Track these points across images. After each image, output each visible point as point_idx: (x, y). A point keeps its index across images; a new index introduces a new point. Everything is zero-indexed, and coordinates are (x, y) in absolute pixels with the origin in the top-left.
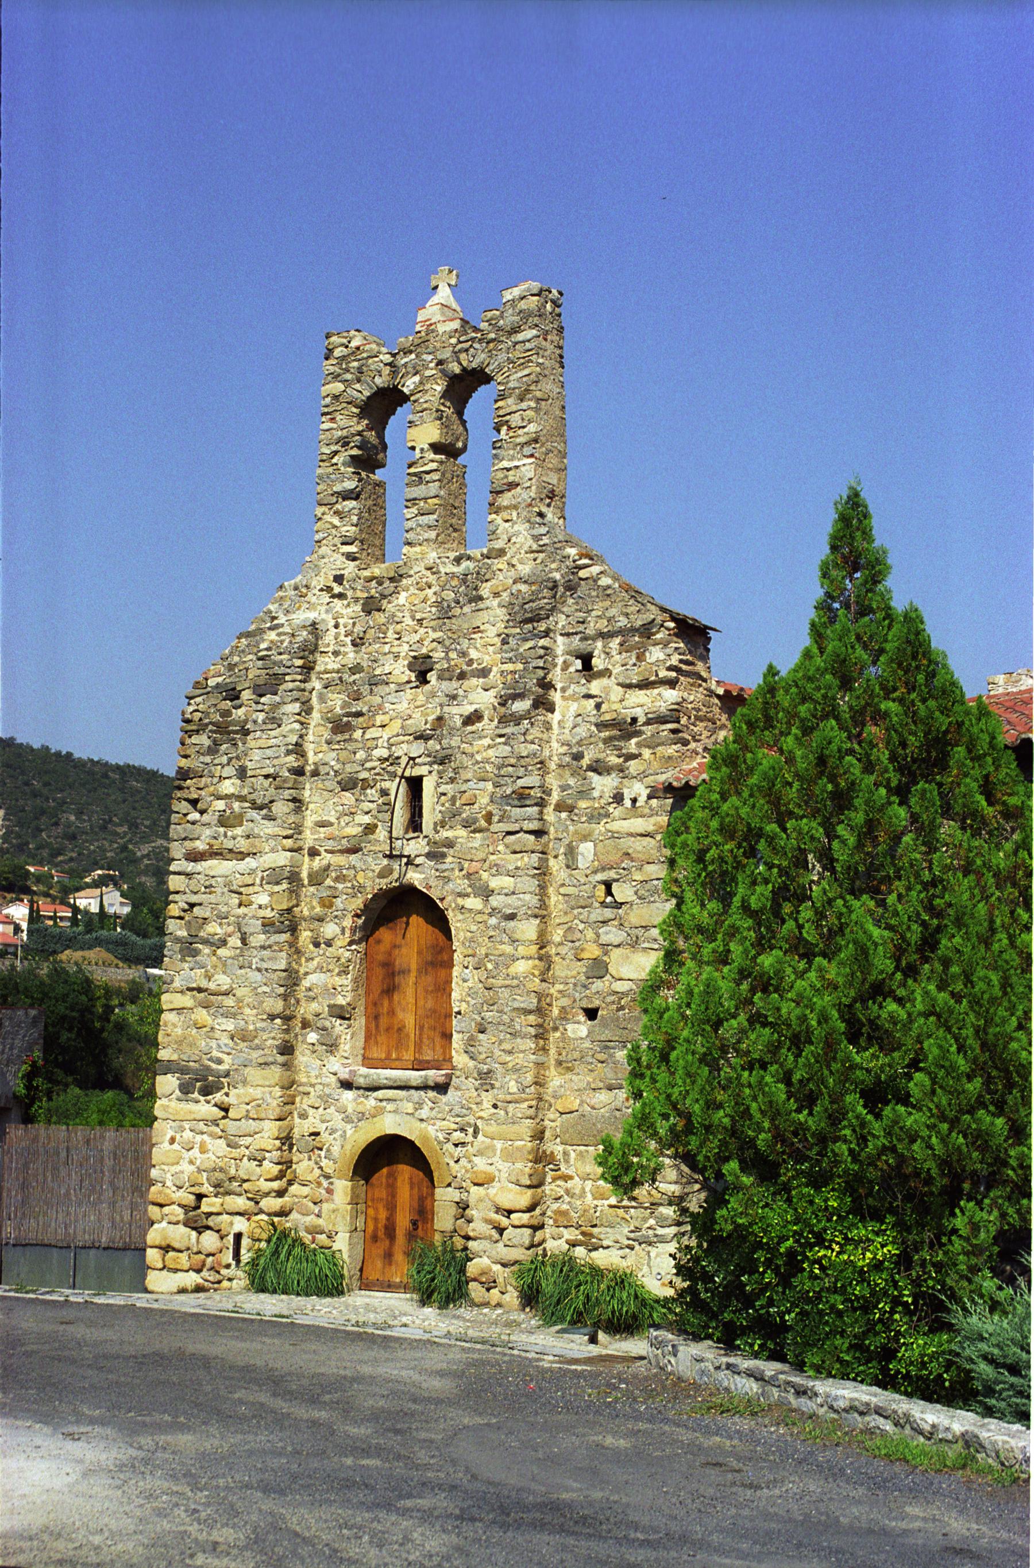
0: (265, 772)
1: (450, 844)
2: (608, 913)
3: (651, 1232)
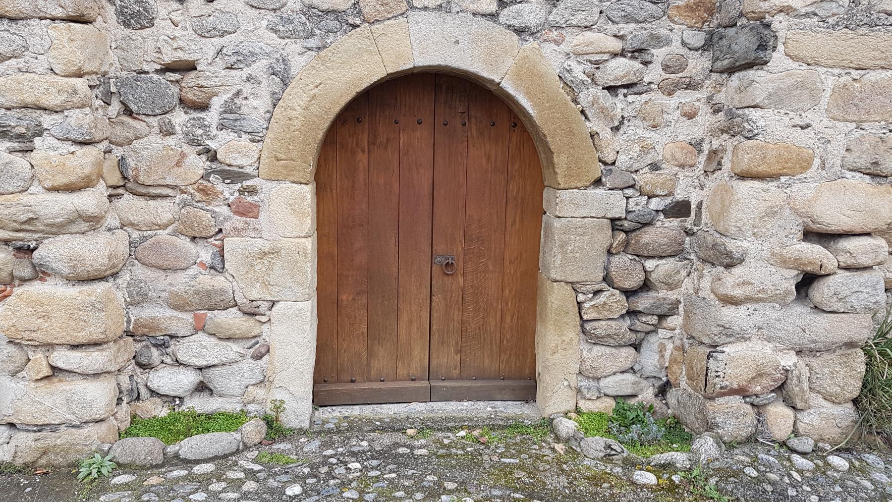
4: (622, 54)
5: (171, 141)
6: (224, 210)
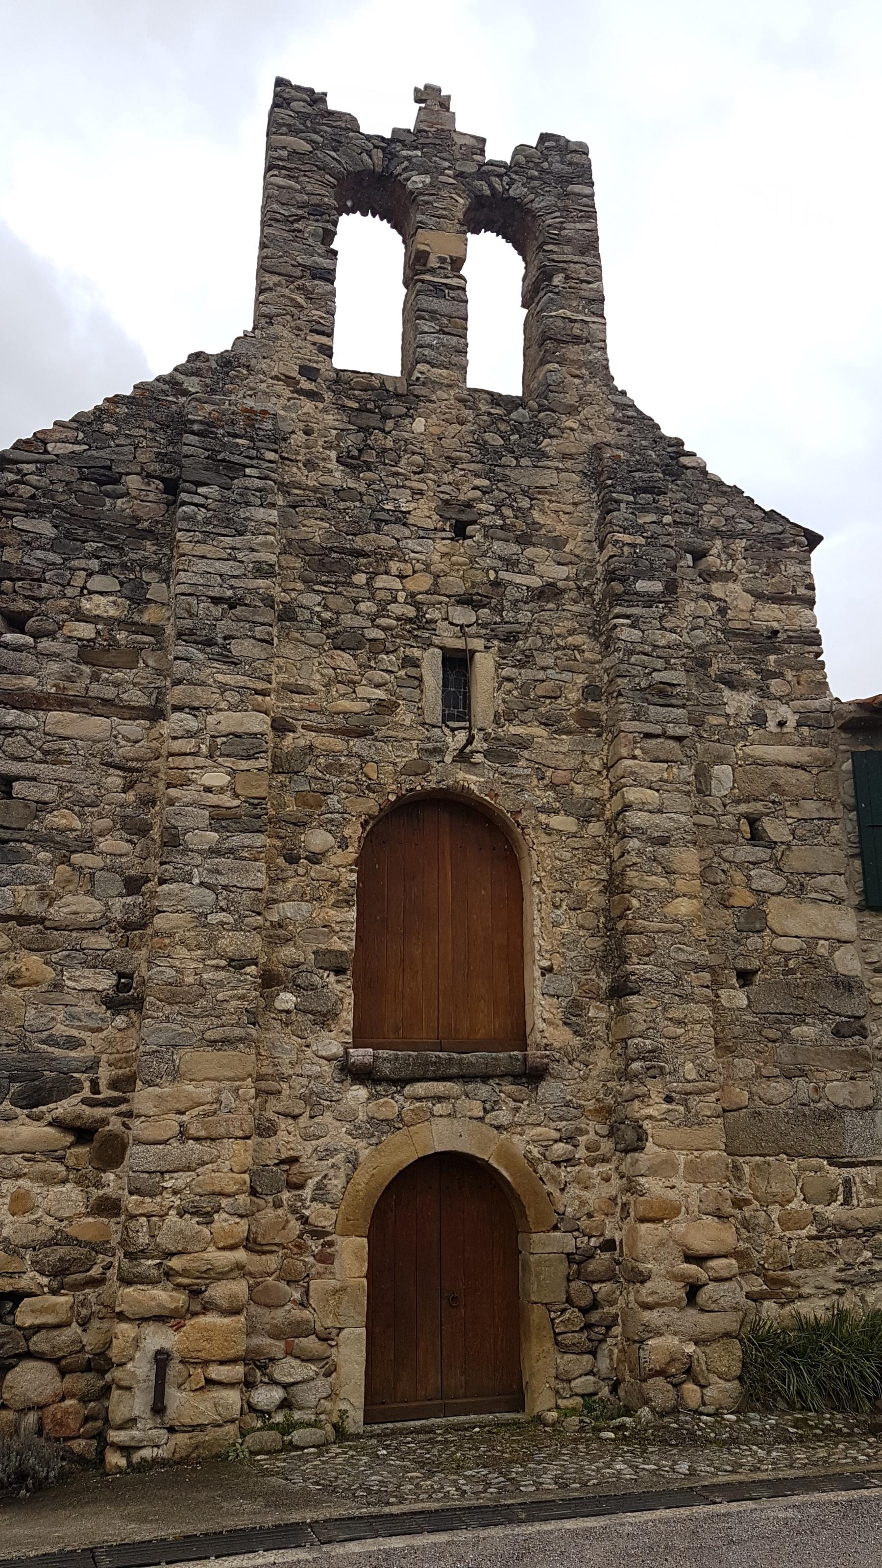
0: (216, 592)
1: (524, 744)
2: (761, 853)
3: (865, 1269)
4: (560, 1140)
5: (280, 1212)
6: (311, 1259)
